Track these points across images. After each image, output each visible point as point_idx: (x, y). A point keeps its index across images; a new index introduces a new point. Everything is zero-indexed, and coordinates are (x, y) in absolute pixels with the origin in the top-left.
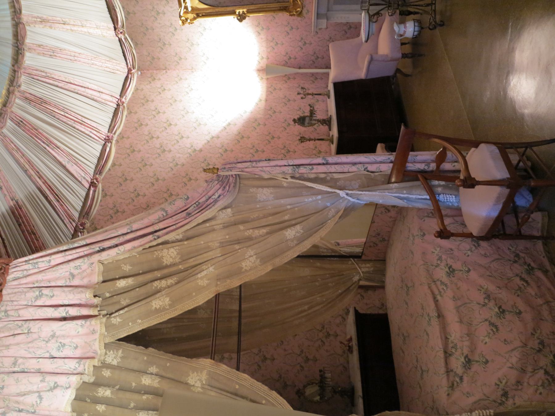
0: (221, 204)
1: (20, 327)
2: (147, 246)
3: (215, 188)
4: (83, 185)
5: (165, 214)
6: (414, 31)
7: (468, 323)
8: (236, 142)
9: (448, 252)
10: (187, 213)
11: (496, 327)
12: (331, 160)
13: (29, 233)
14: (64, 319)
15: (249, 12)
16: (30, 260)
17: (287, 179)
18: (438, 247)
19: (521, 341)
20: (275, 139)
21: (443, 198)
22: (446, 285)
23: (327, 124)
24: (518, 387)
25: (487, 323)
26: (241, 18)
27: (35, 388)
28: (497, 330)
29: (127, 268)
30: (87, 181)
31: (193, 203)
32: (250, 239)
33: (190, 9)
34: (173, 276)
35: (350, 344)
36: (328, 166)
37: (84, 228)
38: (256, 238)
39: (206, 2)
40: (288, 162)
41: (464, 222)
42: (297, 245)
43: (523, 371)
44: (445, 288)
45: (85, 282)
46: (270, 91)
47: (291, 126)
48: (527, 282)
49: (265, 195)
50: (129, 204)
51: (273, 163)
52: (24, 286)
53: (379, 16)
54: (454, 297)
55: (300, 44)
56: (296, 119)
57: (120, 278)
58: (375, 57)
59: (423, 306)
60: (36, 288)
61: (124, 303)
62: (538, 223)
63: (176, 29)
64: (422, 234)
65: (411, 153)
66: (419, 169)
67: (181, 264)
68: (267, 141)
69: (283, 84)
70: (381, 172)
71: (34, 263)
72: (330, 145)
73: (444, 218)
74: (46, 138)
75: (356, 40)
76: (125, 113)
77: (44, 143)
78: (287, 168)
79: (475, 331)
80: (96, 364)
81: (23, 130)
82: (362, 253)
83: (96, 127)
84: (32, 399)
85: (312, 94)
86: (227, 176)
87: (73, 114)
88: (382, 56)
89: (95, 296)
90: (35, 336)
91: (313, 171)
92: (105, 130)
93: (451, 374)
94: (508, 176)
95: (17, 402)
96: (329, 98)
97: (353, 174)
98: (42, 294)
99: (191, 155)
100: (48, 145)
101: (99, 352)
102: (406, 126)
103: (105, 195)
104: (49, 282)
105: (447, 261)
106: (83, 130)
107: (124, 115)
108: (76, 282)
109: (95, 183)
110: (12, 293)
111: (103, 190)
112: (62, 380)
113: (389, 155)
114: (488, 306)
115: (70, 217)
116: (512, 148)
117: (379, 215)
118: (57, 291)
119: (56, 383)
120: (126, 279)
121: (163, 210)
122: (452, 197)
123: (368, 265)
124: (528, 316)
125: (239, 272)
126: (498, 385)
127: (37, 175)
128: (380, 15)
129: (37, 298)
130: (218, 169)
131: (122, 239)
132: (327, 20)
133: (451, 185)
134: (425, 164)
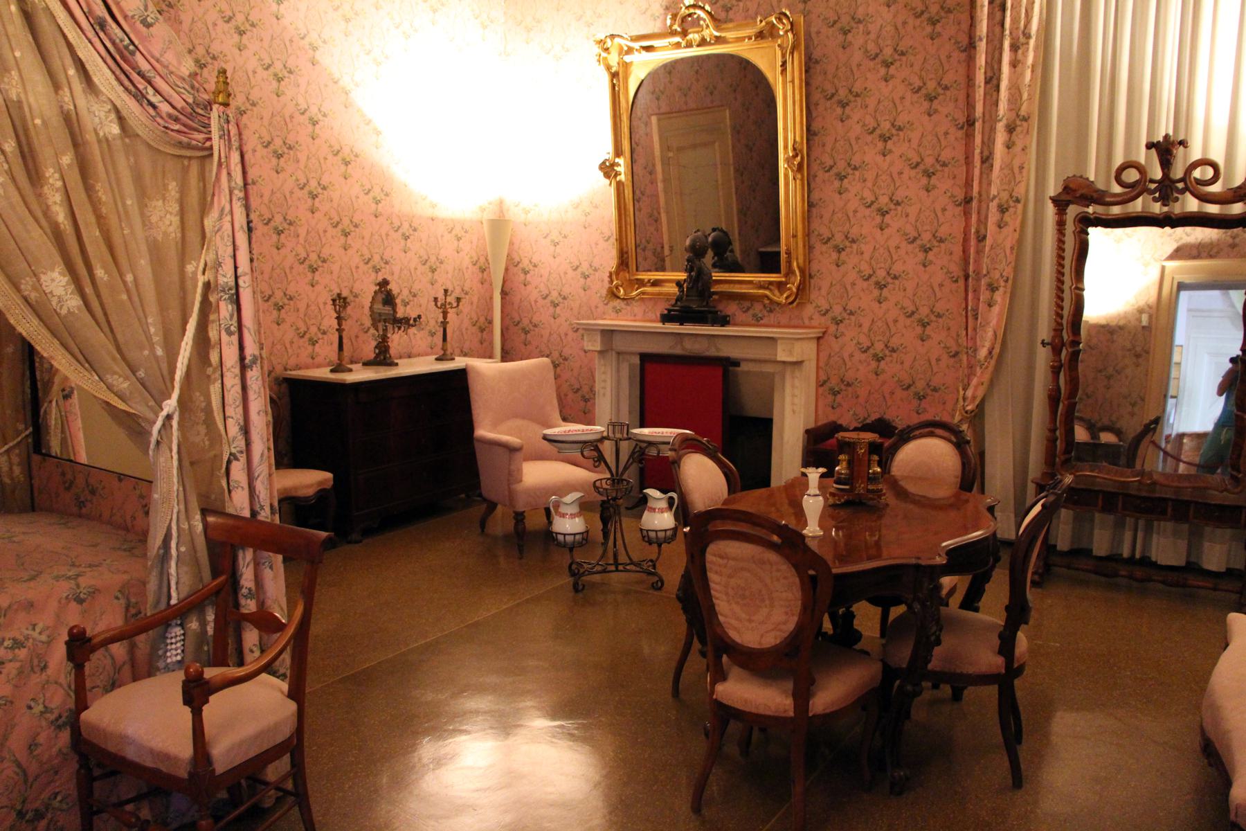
0: (130, 106)
3: (175, 95)
6: (565, 535)
8: (337, 147)
9: (36, 662)
10: (105, 21)
12: (254, 375)
15: (620, 186)
17: (204, 273)
18: (49, 637)
20: (343, 239)
21: (173, 635)
23: (377, 355)
26: (608, 169)
33: (627, 59)
36: (237, 371)
38: (39, 196)
39: (639, 95)
40: (245, 274)
42: (26, 299)
46: (456, 230)
47: (373, 275)
53: (595, 462)
55: (554, 294)
56: (389, 287)
58: (519, 455)
63: (589, 25)
64: (82, 596)
65: (280, 557)
66: (241, 575)
68: (336, 219)
69: (471, 258)
70: (230, 491)
72: (328, 365)
75: (557, 415)
78: (231, 273)
85: (444, 324)
86: (207, 126)
88: (520, 470)
91: (223, 333)
96: (437, 359)
97: (221, 427)
99: (303, 38)
102: (329, 544)
116: (293, 765)
117: (138, 492)
122: (177, 655)
123: (17, 470)
128: (597, 464)
130: (226, 105)
132: (600, 352)
134: (253, 588)
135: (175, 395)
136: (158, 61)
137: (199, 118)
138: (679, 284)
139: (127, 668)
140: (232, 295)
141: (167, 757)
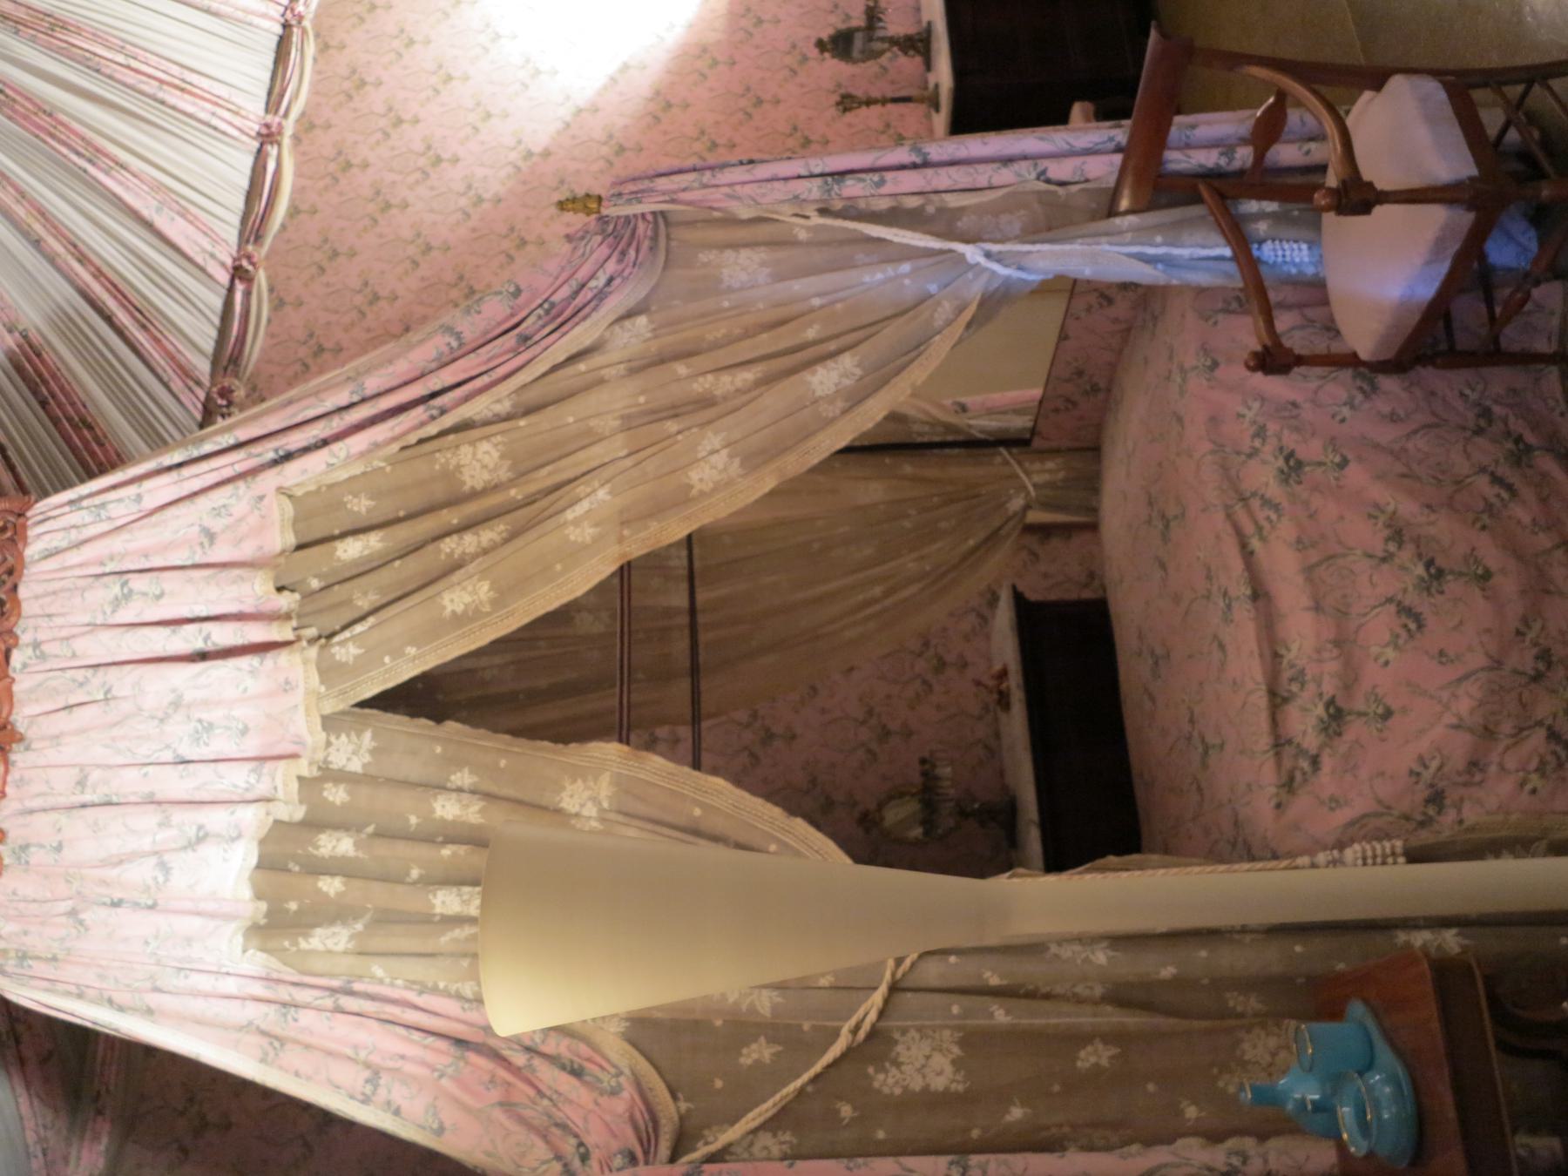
1: (81, 685)
2: (413, 439)
3: (595, 256)
4: (210, 276)
5: (455, 344)
7: (1339, 610)
11: (1417, 618)
12: (936, 151)
13: (75, 427)
14: (203, 656)
16: (82, 498)
17: (807, 217)
18: (1256, 400)
19: (1487, 654)
21: (1272, 254)
22: (1276, 507)
23: (918, 52)
24: (1473, 776)
25: (1392, 608)
27: (146, 844)
28: (1420, 626)
29: (361, 506)
30: (223, 265)
31: (533, 306)
32: (706, 402)
34: (496, 521)
35: (1004, 686)
36: (929, 172)
37: (230, 404)
38: (725, 398)
40: (807, 165)
41: (1332, 320)
42: (845, 412)
43: (1488, 733)
44: (1274, 517)
45: (247, 551)
48: (1510, 488)
49: (744, 269)
50: (353, 324)
51: (762, 171)
52: (78, 572)
54: (1299, 541)
57: (344, 535)
59: (1209, 569)
60: (111, 578)
61: (364, 604)
62: (1552, 313)
64: (1209, 363)
65: (1178, 119)
66: (1201, 166)
67: (514, 486)
68: (740, 115)
70: (1087, 181)
71: (95, 506)
72: (928, 117)
73: (1275, 313)
74: (83, 139)
76: (311, 49)
77: (78, 153)
78: (806, 183)
79: (1356, 632)
80: (305, 773)
81: (10, 118)
82: (1033, 431)
83: (226, 96)
84: (140, 873)
86: (627, 219)
87: (153, 59)
89: (280, 589)
90: (126, 707)
91: (884, 190)
92: (254, 106)
93: (1288, 751)
94: (1473, 171)
95: (104, 882)
97: (1001, 192)
98: (131, 591)
100: (90, 161)
101: (309, 740)
103: (278, 305)
104: (146, 556)
105: (1280, 439)
106: (190, 109)
107: (305, 53)
108: (221, 553)
109: (247, 271)
110: (47, 594)
111: (271, 290)
112: (216, 819)
113: (1111, 128)
114: (1397, 561)
115: (185, 372)
116: (1485, 85)
117: (1083, 315)
118: (170, 581)
119: (200, 828)
120: (361, 536)
121: (449, 330)
122: (1300, 249)
123: (1050, 465)
124: (1508, 584)
125: (683, 498)
126: (1418, 774)
127: (73, 254)
129: (116, 603)
130: (599, 199)
131: (337, 424)
133: (1296, 213)
134: (1220, 149)
135: (960, 247)
136: (557, 278)
137: (619, 227)
139: (1310, 313)
140: (833, 180)
141: (1439, 244)
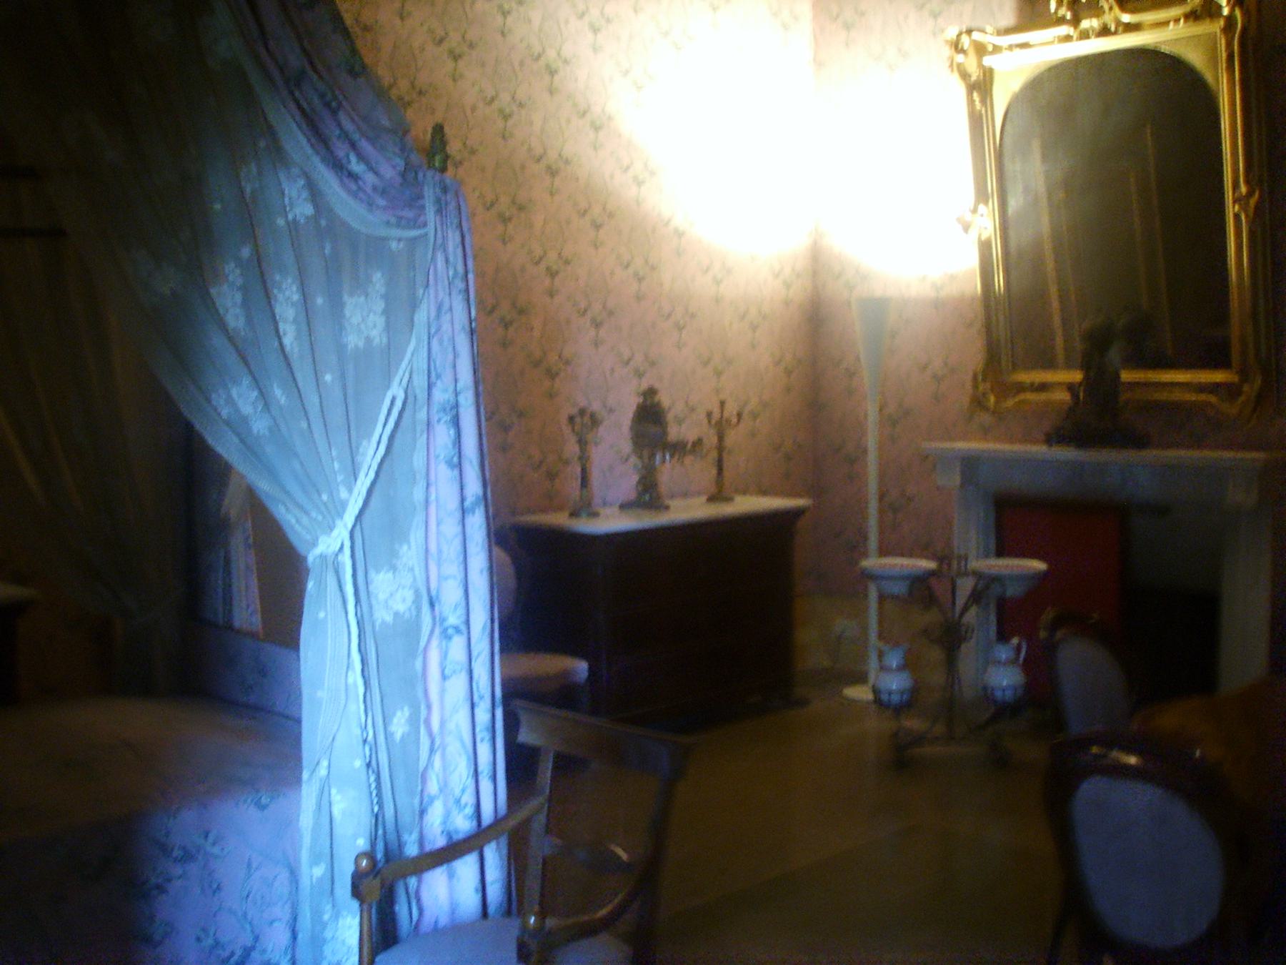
23: (641, 494)
138: (1071, 387)
